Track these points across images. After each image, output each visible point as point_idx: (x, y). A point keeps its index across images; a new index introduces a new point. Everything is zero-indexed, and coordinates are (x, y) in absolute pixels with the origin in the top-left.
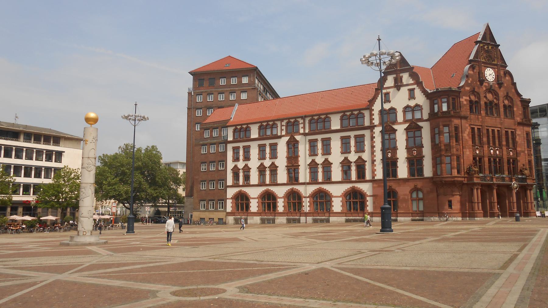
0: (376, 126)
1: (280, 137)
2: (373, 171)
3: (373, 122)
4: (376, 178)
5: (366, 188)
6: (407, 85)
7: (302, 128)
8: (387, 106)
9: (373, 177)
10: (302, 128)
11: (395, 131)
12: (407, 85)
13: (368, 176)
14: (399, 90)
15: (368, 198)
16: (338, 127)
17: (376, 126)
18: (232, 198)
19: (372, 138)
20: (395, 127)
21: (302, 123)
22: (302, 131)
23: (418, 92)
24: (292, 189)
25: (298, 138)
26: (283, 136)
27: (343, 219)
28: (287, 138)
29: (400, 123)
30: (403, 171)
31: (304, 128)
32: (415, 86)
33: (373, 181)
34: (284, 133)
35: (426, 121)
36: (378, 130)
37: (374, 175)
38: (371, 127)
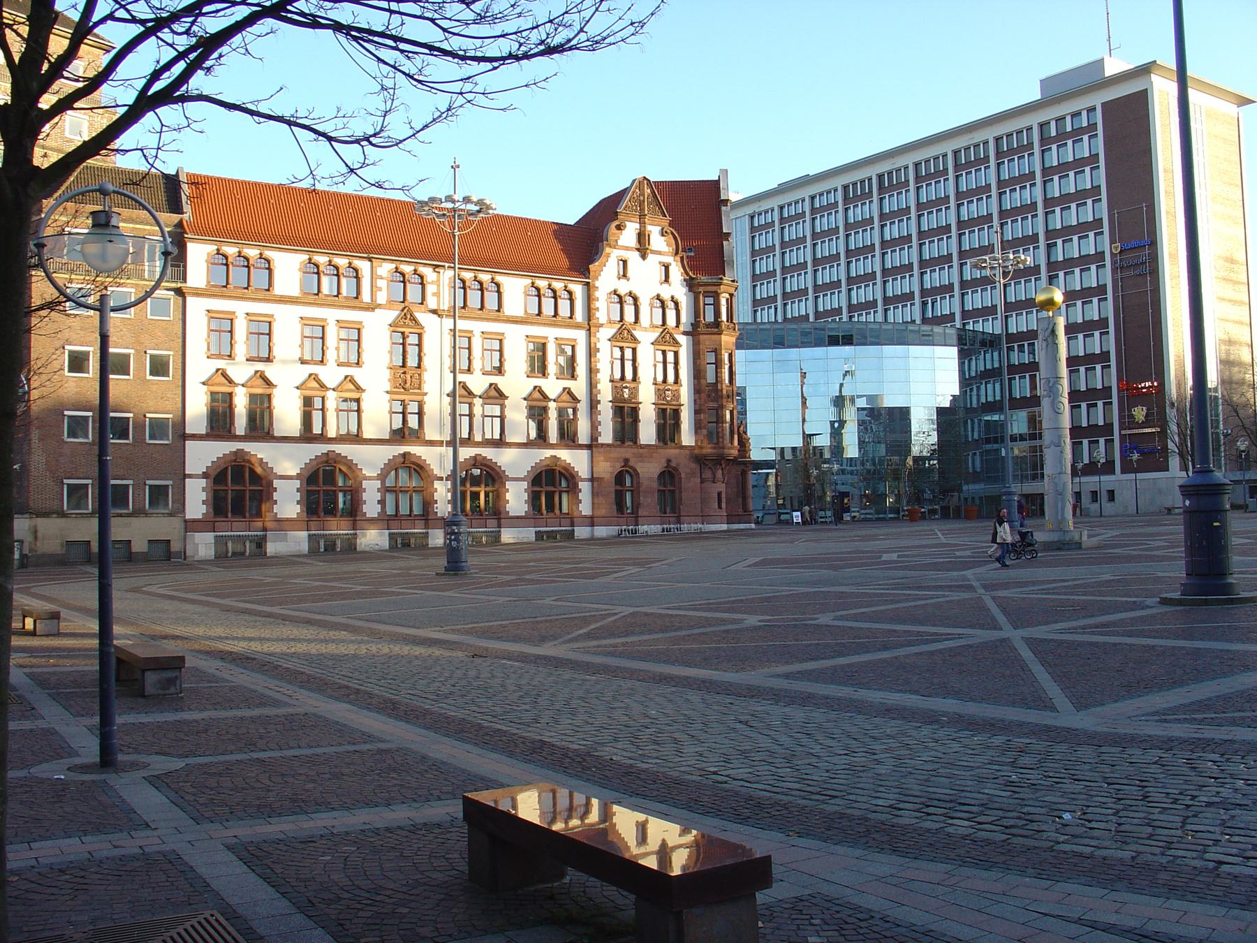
0: (602, 325)
1: (372, 307)
2: (594, 426)
3: (598, 314)
4: (601, 440)
5: (577, 460)
6: (659, 253)
7: (434, 294)
8: (623, 287)
9: (594, 436)
10: (434, 294)
11: (635, 340)
12: (659, 253)
13: (583, 438)
14: (644, 257)
15: (581, 485)
16: (520, 313)
17: (602, 325)
18: (205, 475)
19: (592, 352)
20: (636, 333)
21: (432, 283)
22: (432, 303)
23: (676, 273)
24: (405, 455)
25: (420, 316)
26: (379, 306)
27: (528, 534)
28: (392, 315)
29: (645, 329)
30: (647, 433)
31: (437, 294)
32: (669, 259)
33: (592, 446)
34: (382, 298)
35: (685, 333)
36: (604, 335)
37: (594, 436)
38: (590, 325)
